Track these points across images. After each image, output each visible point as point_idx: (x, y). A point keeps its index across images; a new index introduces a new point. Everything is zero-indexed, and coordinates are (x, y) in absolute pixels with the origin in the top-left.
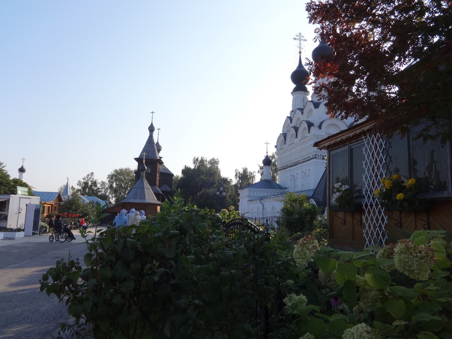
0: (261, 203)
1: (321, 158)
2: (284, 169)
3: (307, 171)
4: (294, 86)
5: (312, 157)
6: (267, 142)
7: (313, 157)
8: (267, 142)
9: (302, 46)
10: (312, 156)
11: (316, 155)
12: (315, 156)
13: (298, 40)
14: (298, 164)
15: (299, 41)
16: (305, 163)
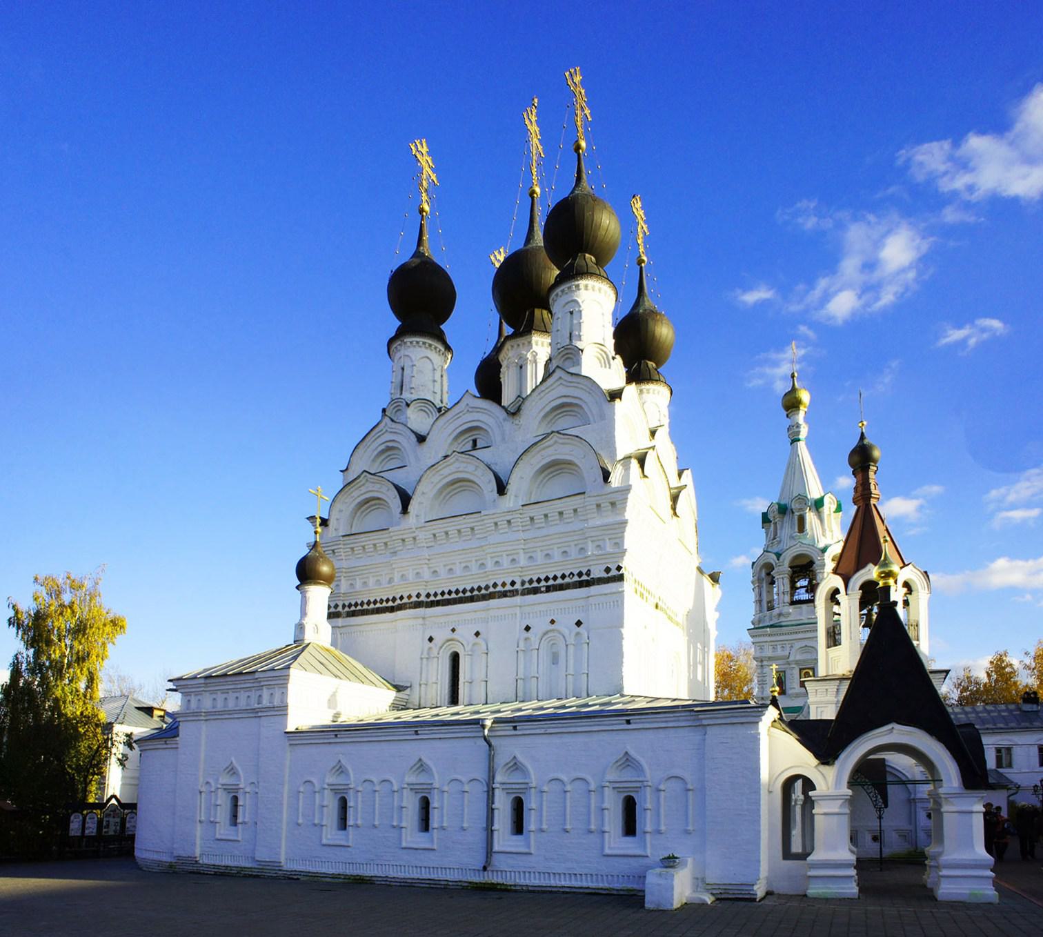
3: (566, 624)
5: (605, 575)
10: (608, 570)
14: (491, 596)
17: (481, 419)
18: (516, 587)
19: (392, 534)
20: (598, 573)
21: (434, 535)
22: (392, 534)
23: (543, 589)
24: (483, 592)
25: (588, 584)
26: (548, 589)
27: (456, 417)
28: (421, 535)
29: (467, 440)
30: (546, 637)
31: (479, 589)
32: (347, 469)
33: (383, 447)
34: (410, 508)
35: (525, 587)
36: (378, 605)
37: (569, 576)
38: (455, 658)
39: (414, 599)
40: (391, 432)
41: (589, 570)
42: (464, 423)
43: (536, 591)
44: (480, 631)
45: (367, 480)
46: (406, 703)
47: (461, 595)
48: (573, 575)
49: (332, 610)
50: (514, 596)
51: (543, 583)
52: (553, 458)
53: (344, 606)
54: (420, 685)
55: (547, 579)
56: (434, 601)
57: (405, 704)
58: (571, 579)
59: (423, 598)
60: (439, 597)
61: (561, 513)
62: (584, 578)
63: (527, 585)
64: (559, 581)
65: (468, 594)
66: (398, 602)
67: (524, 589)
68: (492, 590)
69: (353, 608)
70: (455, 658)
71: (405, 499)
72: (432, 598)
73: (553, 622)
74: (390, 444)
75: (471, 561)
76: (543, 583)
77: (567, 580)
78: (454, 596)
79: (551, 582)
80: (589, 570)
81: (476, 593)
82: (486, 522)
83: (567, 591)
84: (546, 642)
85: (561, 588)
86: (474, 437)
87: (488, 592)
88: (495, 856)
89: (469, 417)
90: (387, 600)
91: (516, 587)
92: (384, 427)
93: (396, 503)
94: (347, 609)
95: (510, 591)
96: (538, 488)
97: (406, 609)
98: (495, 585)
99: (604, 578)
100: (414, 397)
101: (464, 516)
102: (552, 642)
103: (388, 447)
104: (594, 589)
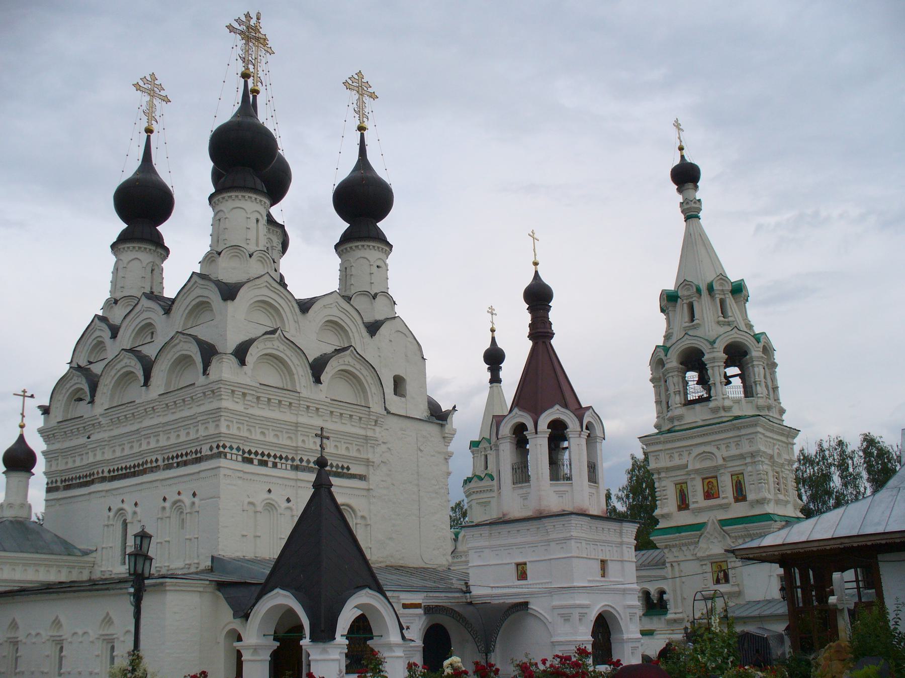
1: (240, 458)
4: (121, 226)
5: (209, 453)
7: (215, 451)
9: (157, 114)
10: (211, 449)
11: (224, 447)
12: (221, 449)
13: (146, 94)
14: (144, 472)
19: (86, 420)
20: (206, 451)
22: (86, 420)
23: (175, 465)
25: (198, 460)
26: (178, 465)
28: (103, 421)
29: (147, 334)
33: (95, 342)
34: (97, 399)
45: (73, 376)
49: (50, 485)
53: (62, 481)
55: (177, 456)
59: (106, 474)
62: (199, 455)
76: (175, 460)
77: (189, 457)
79: (180, 459)
82: (139, 409)
85: (185, 463)
89: (145, 315)
94: (64, 484)
96: (176, 377)
103: (98, 341)
104: (204, 466)
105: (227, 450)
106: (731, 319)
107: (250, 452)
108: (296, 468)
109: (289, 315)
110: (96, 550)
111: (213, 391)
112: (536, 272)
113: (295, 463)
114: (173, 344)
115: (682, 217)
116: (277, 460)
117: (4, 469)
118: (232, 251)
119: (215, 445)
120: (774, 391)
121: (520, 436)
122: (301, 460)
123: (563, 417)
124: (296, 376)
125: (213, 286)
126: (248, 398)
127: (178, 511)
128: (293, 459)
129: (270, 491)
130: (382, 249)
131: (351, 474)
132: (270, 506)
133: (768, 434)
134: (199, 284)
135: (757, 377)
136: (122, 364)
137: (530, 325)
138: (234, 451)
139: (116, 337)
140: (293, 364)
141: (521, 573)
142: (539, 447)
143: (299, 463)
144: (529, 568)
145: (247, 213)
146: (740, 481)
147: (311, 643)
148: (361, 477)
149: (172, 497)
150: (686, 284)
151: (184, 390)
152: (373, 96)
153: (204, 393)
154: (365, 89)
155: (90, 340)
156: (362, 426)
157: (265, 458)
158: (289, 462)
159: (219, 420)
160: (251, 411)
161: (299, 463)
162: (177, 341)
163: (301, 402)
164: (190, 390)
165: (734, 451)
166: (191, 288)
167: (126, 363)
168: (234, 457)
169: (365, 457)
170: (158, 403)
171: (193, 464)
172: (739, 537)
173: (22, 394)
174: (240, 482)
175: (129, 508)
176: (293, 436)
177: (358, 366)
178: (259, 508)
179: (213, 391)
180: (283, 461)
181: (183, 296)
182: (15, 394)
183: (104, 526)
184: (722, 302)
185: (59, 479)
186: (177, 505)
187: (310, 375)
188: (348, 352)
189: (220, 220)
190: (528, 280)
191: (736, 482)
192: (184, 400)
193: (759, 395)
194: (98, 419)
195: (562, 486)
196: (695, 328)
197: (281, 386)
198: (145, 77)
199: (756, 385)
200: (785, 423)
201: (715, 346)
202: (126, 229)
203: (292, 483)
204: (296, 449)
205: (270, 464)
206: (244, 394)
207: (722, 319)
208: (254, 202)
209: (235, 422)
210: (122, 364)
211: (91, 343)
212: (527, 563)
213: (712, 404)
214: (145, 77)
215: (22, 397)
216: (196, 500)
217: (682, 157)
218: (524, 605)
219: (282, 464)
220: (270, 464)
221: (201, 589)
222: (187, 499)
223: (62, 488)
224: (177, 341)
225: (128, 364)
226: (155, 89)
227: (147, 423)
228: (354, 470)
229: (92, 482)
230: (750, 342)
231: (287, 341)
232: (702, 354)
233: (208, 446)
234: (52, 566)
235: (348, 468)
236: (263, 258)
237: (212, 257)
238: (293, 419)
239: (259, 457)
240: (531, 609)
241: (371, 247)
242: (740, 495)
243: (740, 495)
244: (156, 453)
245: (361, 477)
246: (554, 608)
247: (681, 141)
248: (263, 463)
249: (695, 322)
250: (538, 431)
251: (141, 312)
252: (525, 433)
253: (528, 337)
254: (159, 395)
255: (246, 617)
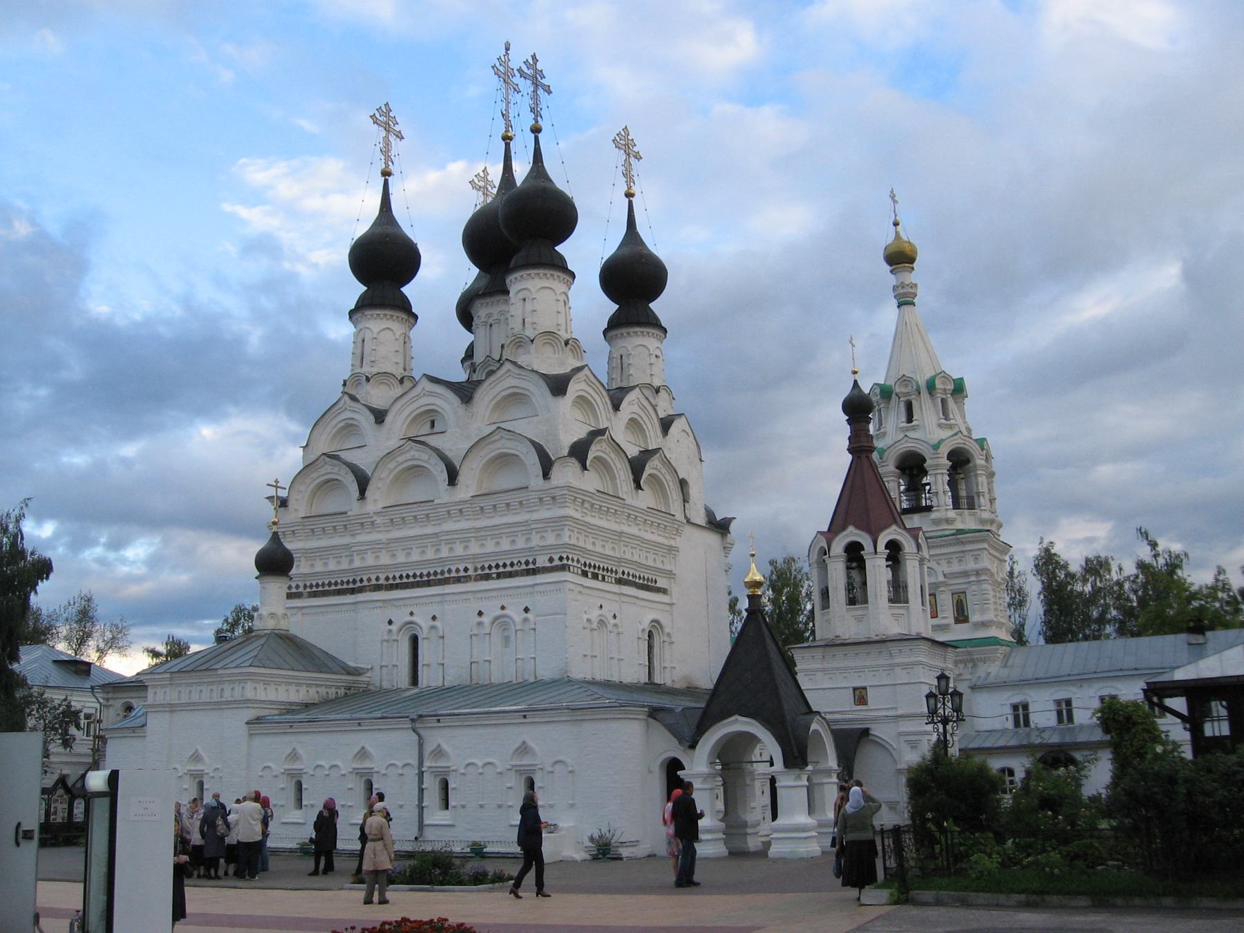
0: (414, 731)
1: (580, 572)
2: (314, 595)
6: (277, 481)
7: (557, 562)
8: (277, 481)
10: (551, 560)
11: (568, 558)
12: (565, 562)
15: (384, 133)
16: (491, 582)
17: (436, 403)
18: (469, 573)
19: (351, 518)
20: (542, 561)
21: (392, 520)
23: (494, 576)
24: (439, 577)
25: (534, 572)
26: (499, 576)
27: (412, 401)
28: (379, 520)
29: (426, 421)
30: (498, 621)
31: (435, 573)
32: (307, 445)
33: (342, 424)
35: (478, 573)
36: (339, 587)
37: (517, 564)
38: (415, 641)
39: (374, 582)
40: (350, 410)
41: (535, 559)
42: (421, 406)
43: (487, 577)
44: (437, 616)
45: (325, 463)
46: (368, 685)
47: (418, 579)
48: (521, 564)
50: (467, 582)
51: (494, 570)
52: (498, 452)
53: (305, 587)
54: (381, 667)
55: (497, 566)
56: (393, 584)
57: (366, 686)
58: (519, 567)
59: (382, 582)
60: (398, 581)
61: (508, 505)
62: (531, 566)
63: (479, 572)
64: (509, 569)
65: (425, 578)
66: (358, 584)
67: (477, 575)
68: (447, 575)
69: (314, 589)
70: (415, 641)
71: (363, 483)
72: (391, 582)
73: (503, 608)
74: (350, 422)
75: (427, 546)
76: (494, 570)
77: (516, 568)
78: (411, 580)
79: (501, 570)
80: (535, 559)
81: (432, 577)
82: (439, 510)
83: (517, 578)
84: (497, 627)
85: (510, 575)
86: (432, 418)
87: (443, 577)
88: (426, 829)
89: (425, 400)
90: (348, 582)
91: (469, 573)
92: (344, 405)
93: (354, 489)
94: (308, 590)
95: (463, 577)
97: (365, 591)
98: (450, 571)
99: (548, 567)
100: (375, 370)
101: (419, 504)
102: (505, 627)
103: (347, 423)
104: (540, 578)
105: (570, 562)
106: (952, 422)
107: (585, 564)
108: (620, 582)
109: (603, 412)
110: (372, 668)
111: (554, 498)
112: (856, 381)
113: (618, 576)
114: (490, 440)
115: (895, 303)
116: (605, 573)
117: (257, 573)
118: (545, 338)
119: (556, 557)
120: (991, 503)
121: (854, 554)
122: (623, 573)
123: (898, 537)
124: (618, 481)
125: (536, 378)
126: (586, 505)
127: (500, 627)
128: (616, 572)
129: (601, 607)
130: (653, 334)
131: (657, 587)
132: (602, 623)
133: (992, 551)
134: (513, 373)
135: (980, 488)
136: (408, 456)
137: (850, 438)
138: (575, 564)
139: (383, 421)
140: (616, 467)
141: (859, 697)
142: (878, 570)
143: (621, 576)
144: (870, 692)
145: (556, 294)
146: (961, 601)
147: (785, 770)
148: (663, 591)
149: (492, 611)
150: (905, 380)
151: (510, 493)
152: (638, 157)
153: (541, 499)
154: (631, 148)
155: (334, 422)
156: (667, 535)
157: (596, 571)
158: (613, 575)
159: (563, 529)
160: (589, 519)
161: (621, 576)
162: (496, 438)
163: (625, 510)
164: (521, 496)
165: (956, 568)
166: (501, 377)
167: (414, 456)
168: (576, 569)
169: (668, 568)
170: (469, 506)
171: (523, 575)
172: (960, 661)
173: (275, 484)
174: (580, 597)
175: (422, 620)
176: (616, 547)
177: (663, 471)
178: (595, 626)
179: (554, 498)
180: (609, 574)
181: (490, 384)
182: (268, 485)
183: (383, 641)
184: (944, 401)
185: (301, 585)
186: (502, 622)
187: (631, 480)
188: (658, 455)
189: (524, 300)
190: (846, 391)
191: (958, 601)
192: (508, 505)
193: (982, 508)
194: (372, 517)
195: (899, 609)
196: (914, 429)
197: (603, 491)
198: (380, 107)
199: (979, 496)
200: (1001, 539)
201: (939, 451)
202: (366, 291)
203: (616, 597)
204: (620, 560)
205: (600, 578)
206: (583, 501)
207: (943, 421)
208: (551, 279)
209: (576, 532)
210: (408, 456)
211: (336, 425)
212: (868, 688)
213: (934, 515)
214: (380, 107)
215: (274, 488)
216: (529, 615)
217: (897, 234)
218: (865, 732)
219: (609, 576)
220: (600, 578)
221: (640, 717)
222: (515, 613)
223: (305, 595)
224: (496, 438)
225: (417, 457)
226: (390, 123)
227: (449, 526)
228: (661, 583)
229: (361, 590)
230: (974, 449)
231: (613, 444)
232: (924, 460)
233: (547, 558)
234: (290, 684)
235: (656, 582)
236: (575, 348)
237: (520, 342)
238: (615, 527)
239: (592, 570)
240: (871, 734)
241: (650, 334)
242: (961, 616)
243: (961, 616)
244: (466, 561)
245: (663, 591)
246: (900, 734)
247: (896, 215)
248: (595, 576)
249: (914, 423)
250: (878, 551)
251: (418, 397)
252: (862, 553)
253: (848, 450)
254: (472, 497)
255: (693, 746)
